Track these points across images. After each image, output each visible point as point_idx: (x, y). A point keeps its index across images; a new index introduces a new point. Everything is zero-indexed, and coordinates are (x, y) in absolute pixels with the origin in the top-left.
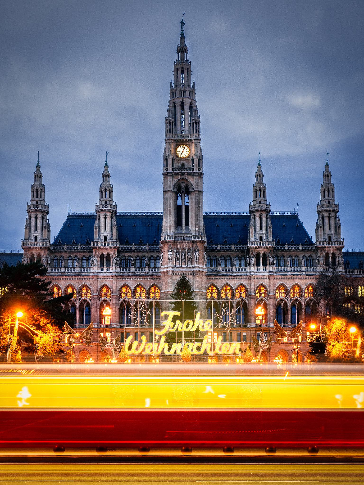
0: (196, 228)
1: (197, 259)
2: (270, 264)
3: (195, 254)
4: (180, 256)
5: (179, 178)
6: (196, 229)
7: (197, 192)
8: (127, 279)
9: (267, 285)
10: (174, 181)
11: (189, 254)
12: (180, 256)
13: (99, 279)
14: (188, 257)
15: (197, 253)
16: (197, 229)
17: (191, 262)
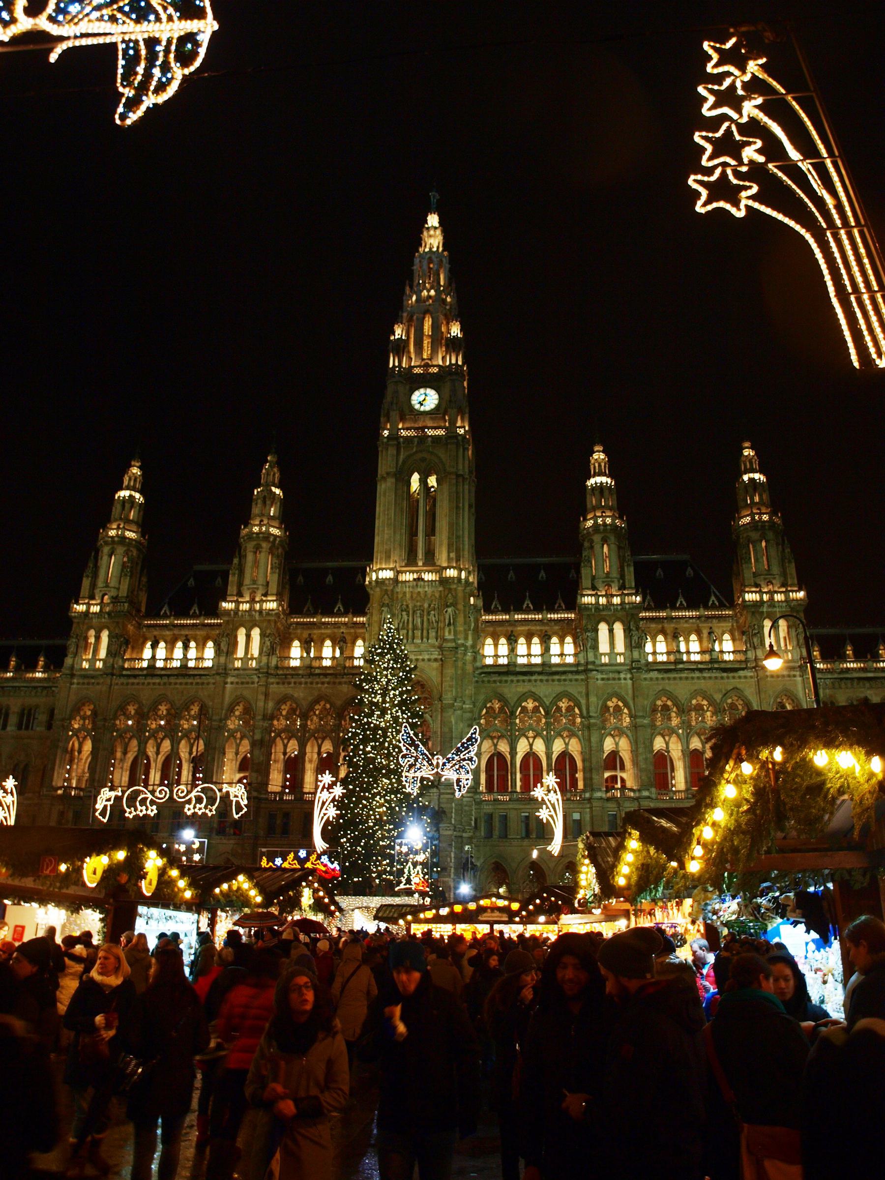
0: (449, 553)
1: (449, 624)
2: (633, 644)
3: (446, 612)
4: (411, 619)
5: (414, 450)
6: (449, 556)
7: (454, 477)
8: (292, 685)
9: (627, 695)
10: (402, 457)
11: (432, 612)
12: (411, 619)
13: (228, 686)
14: (428, 619)
15: (450, 610)
16: (453, 555)
17: (437, 632)
